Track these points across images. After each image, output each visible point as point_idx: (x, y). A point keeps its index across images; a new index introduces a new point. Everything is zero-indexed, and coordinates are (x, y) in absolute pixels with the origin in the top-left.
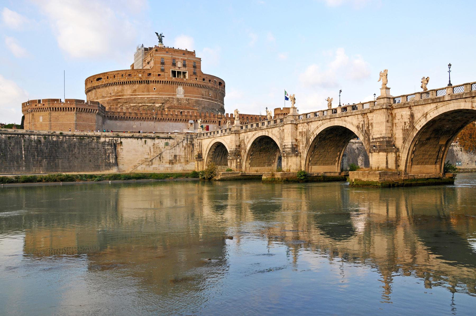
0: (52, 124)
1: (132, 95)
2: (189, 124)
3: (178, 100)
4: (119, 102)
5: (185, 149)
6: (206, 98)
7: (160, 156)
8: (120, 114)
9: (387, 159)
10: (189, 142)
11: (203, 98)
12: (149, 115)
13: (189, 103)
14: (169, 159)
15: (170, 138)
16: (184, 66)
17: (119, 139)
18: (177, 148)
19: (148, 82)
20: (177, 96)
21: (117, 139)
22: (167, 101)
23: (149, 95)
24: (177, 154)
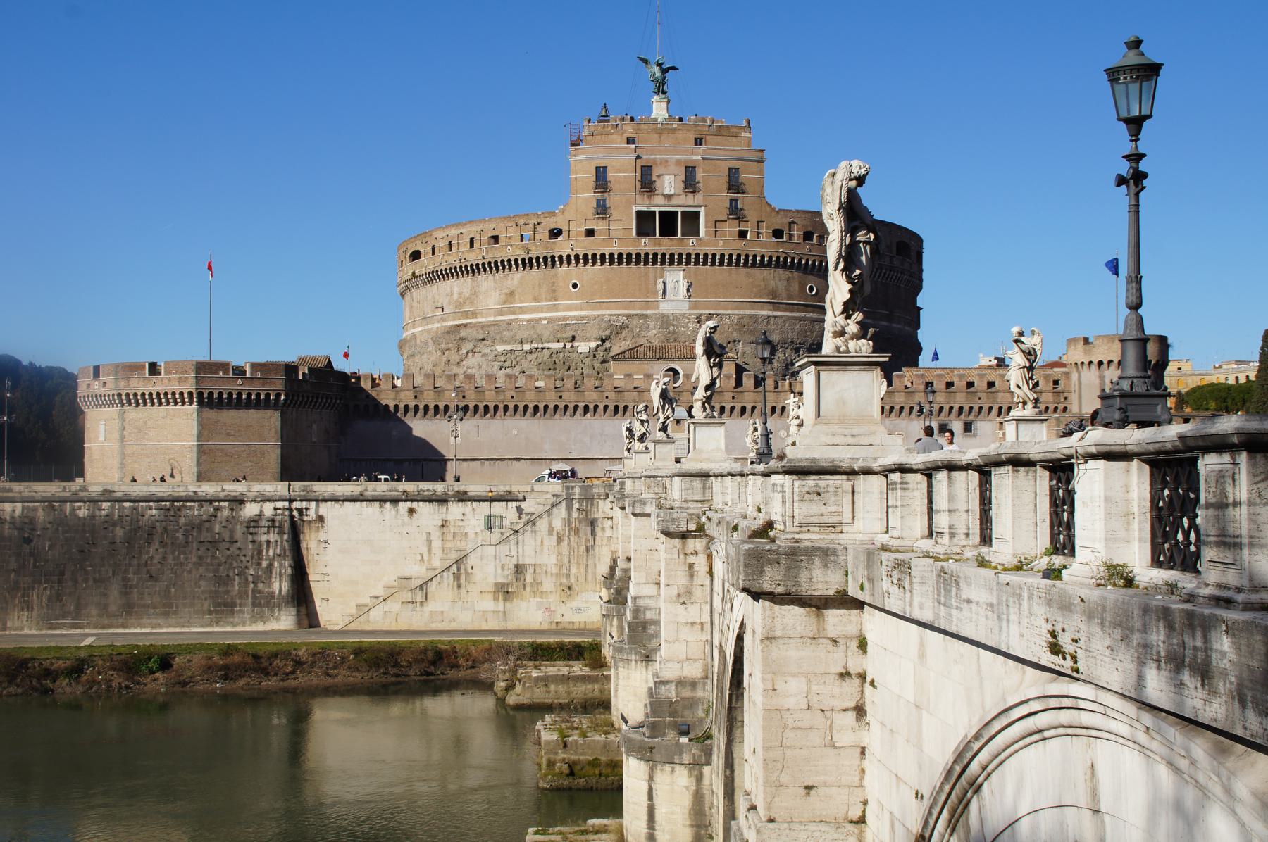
0: (128, 451)
3: (665, 321)
5: (560, 540)
6: (790, 307)
7: (458, 568)
8: (402, 395)
9: (650, 798)
10: (575, 515)
11: (776, 306)
12: (508, 395)
14: (492, 580)
15: (506, 498)
16: (690, 184)
17: (313, 504)
18: (527, 538)
19: (550, 261)
21: (304, 504)
22: (618, 329)
23: (555, 308)
24: (527, 561)
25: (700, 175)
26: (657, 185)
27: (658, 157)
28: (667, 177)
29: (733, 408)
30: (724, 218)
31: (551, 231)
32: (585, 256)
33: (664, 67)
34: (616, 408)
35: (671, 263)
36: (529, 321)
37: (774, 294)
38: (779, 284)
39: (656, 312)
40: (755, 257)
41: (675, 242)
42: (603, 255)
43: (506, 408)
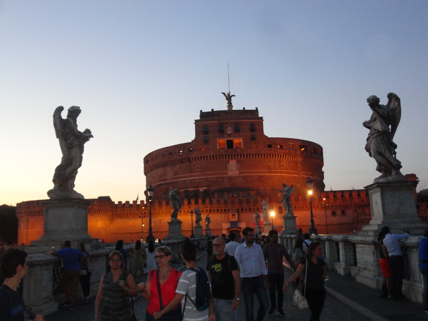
1: (173, 179)
2: (230, 216)
20: (228, 173)
23: (192, 176)
26: (225, 131)
27: (225, 121)
28: (228, 128)
29: (254, 209)
33: (230, 95)
34: (210, 211)
35: (232, 158)
36: (182, 181)
37: (269, 168)
40: (262, 155)
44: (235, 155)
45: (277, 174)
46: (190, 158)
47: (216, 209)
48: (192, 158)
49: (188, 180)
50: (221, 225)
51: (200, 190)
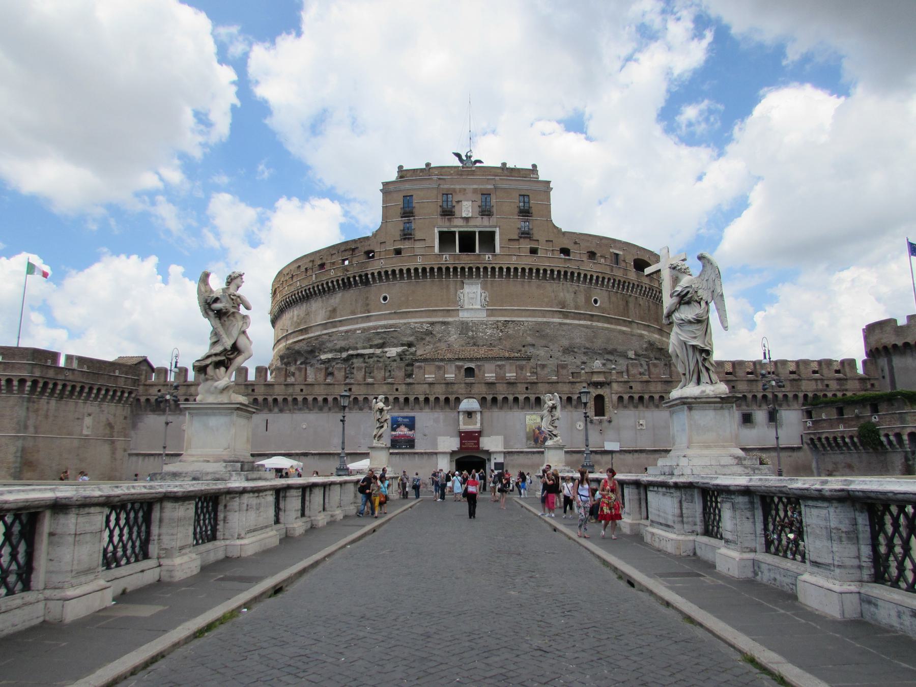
2: (461, 417)
3: (464, 327)
4: (298, 353)
11: (566, 315)
13: (508, 337)
16: (486, 212)
19: (365, 280)
20: (461, 314)
25: (494, 201)
27: (458, 187)
28: (465, 203)
29: (527, 399)
30: (516, 237)
31: (367, 253)
32: (394, 271)
33: (473, 159)
34: (407, 400)
36: (347, 332)
38: (567, 295)
39: (457, 319)
40: (545, 271)
41: (472, 258)
42: (409, 270)
43: (295, 400)
44: (478, 269)
45: (582, 322)
46: (366, 275)
47: (422, 398)
48: (373, 274)
49: (359, 329)
50: (435, 444)
51: (388, 355)
